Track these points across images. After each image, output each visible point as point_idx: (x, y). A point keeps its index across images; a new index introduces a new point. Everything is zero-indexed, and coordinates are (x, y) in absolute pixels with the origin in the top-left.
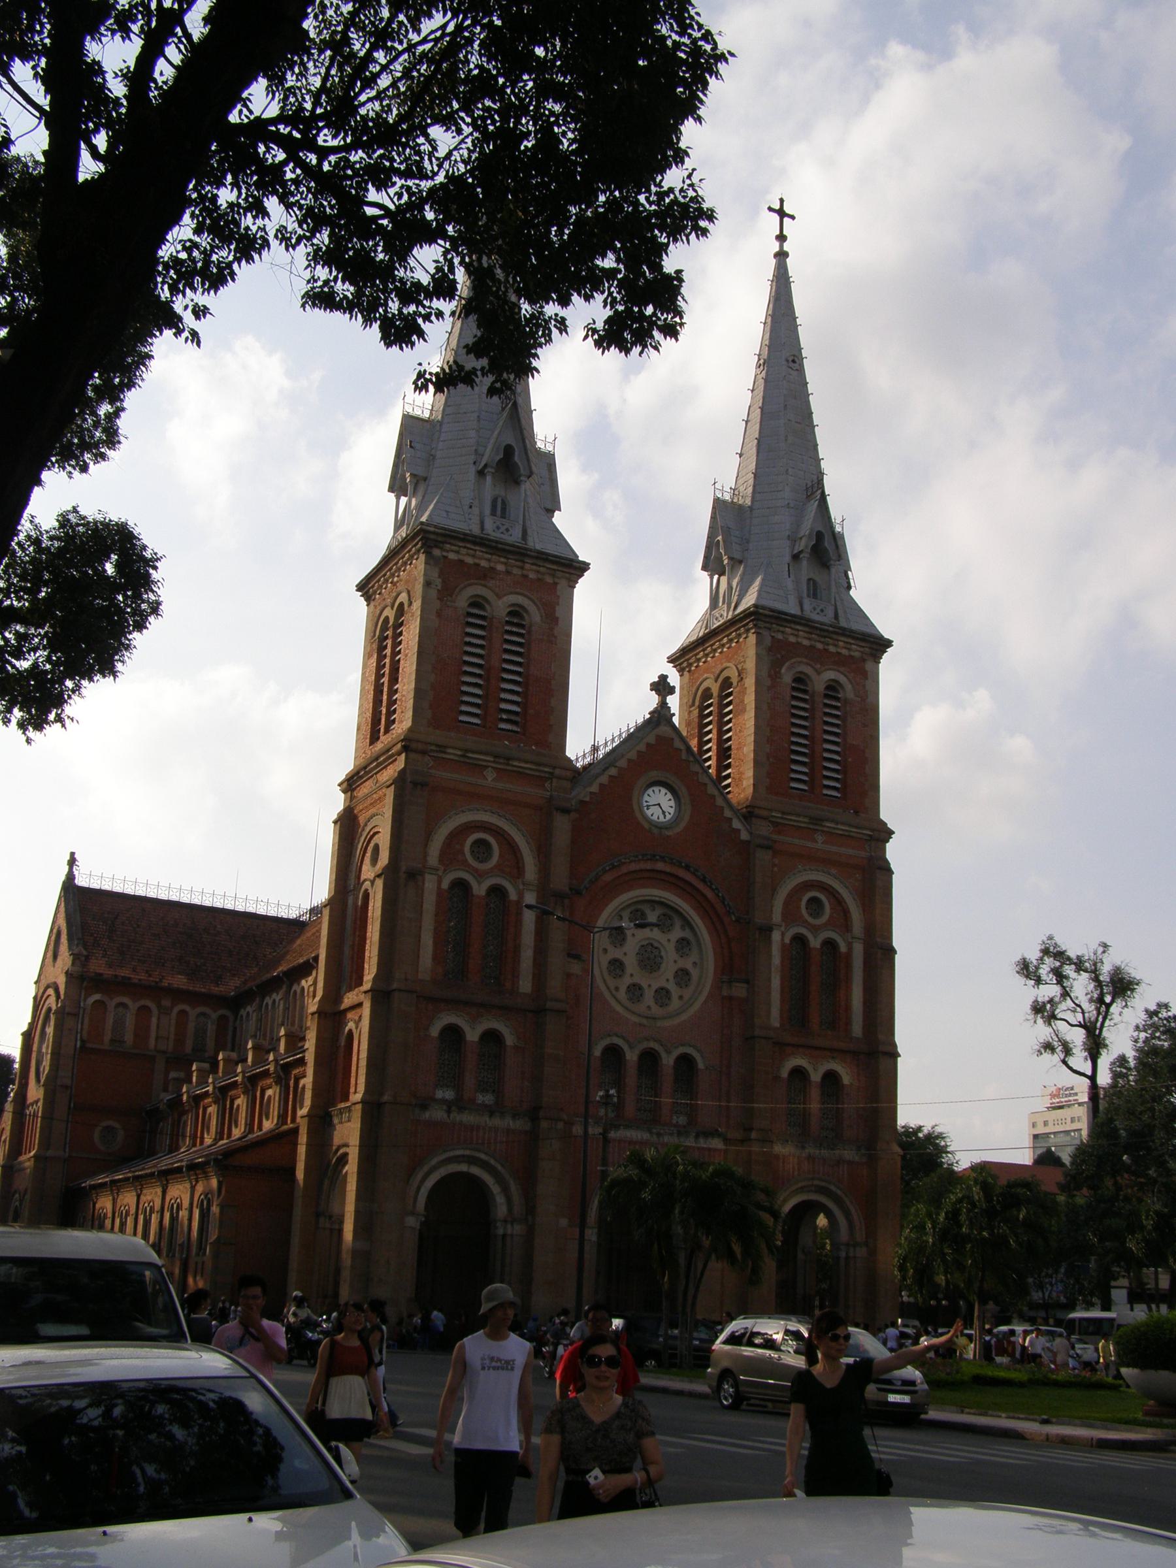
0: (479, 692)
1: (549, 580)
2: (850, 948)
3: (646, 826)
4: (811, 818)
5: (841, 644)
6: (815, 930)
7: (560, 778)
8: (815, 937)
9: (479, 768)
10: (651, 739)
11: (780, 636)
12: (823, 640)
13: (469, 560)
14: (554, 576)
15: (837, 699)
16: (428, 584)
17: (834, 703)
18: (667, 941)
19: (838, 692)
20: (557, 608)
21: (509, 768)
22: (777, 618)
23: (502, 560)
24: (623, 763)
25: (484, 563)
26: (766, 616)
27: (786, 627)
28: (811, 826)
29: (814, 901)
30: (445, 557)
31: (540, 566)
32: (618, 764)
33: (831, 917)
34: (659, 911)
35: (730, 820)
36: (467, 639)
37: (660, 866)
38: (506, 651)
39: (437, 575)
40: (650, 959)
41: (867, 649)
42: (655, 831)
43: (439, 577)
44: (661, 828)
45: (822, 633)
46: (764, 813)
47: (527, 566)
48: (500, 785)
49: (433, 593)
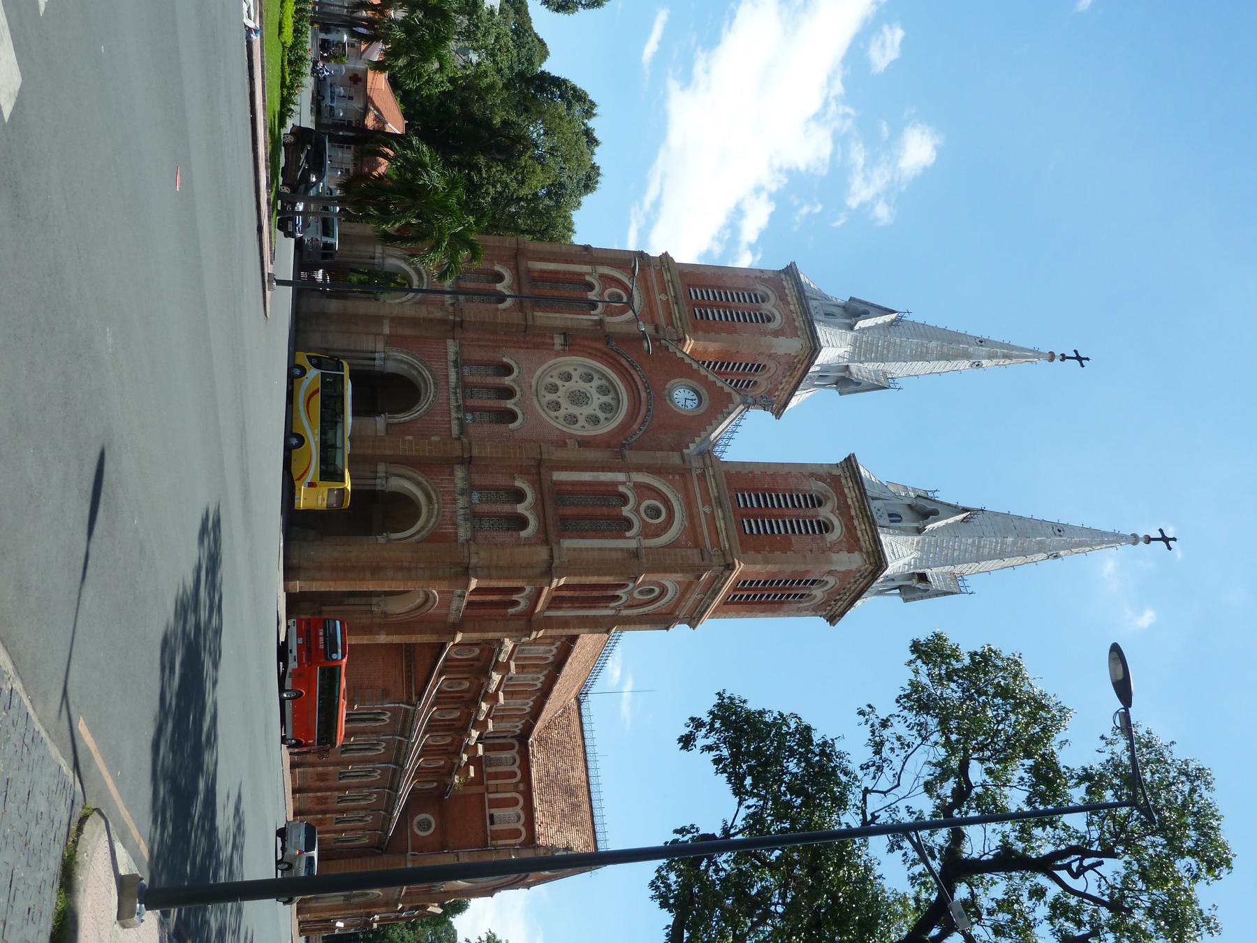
2: (630, 538)
3: (668, 386)
4: (719, 497)
6: (637, 511)
8: (630, 511)
9: (664, 290)
11: (844, 481)
17: (816, 528)
18: (593, 408)
19: (826, 532)
22: (855, 473)
26: (852, 466)
28: (713, 501)
29: (658, 515)
33: (653, 524)
34: (613, 403)
37: (643, 395)
40: (578, 398)
42: (666, 392)
45: (863, 510)
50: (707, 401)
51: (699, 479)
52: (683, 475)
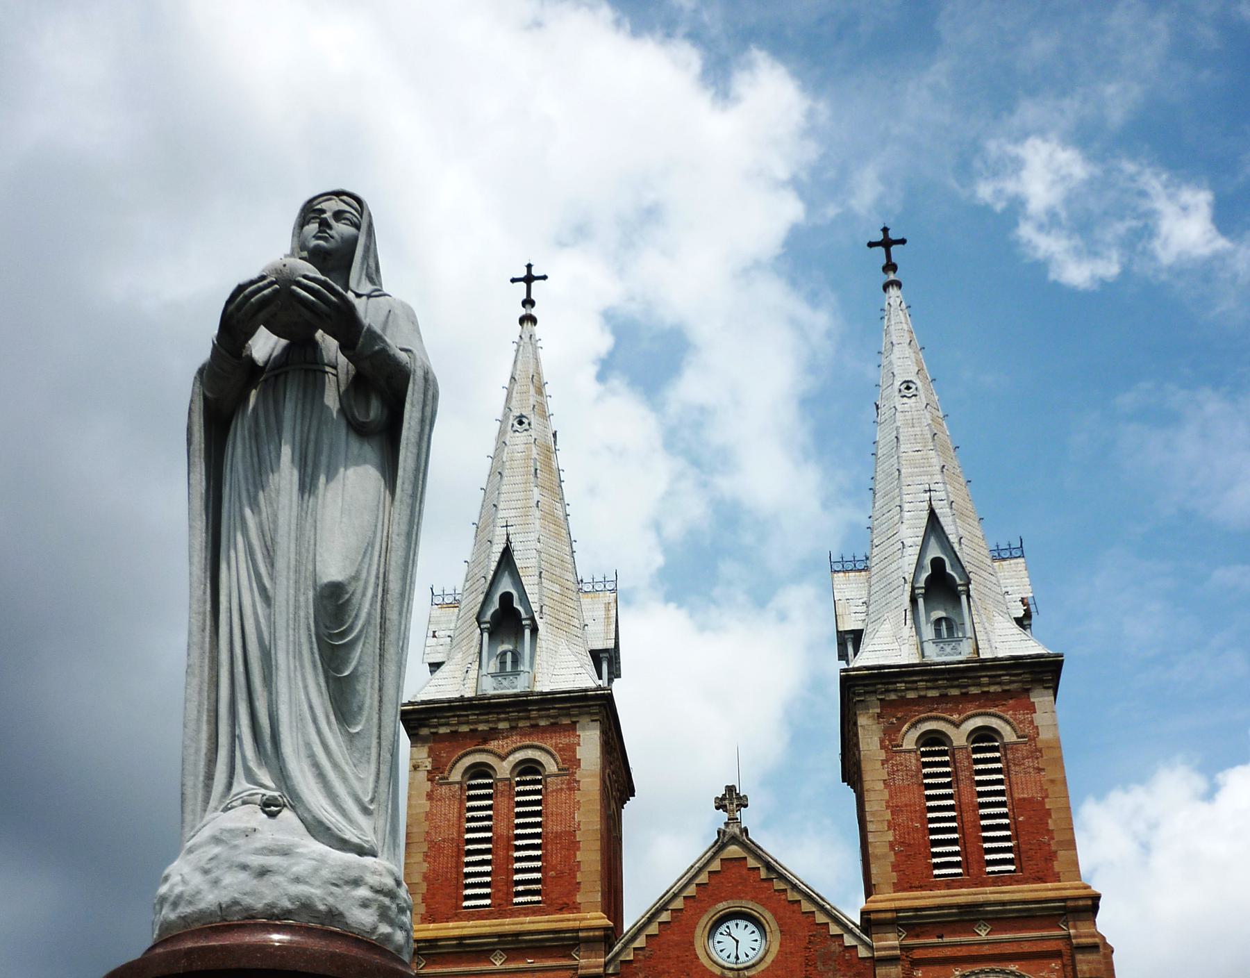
0: (488, 868)
1: (566, 721)
3: (717, 971)
4: (959, 906)
5: (985, 680)
7: (587, 941)
10: (716, 866)
11: (893, 697)
12: (956, 683)
13: (464, 729)
14: (569, 715)
15: (995, 749)
16: (415, 768)
17: (989, 755)
20: (577, 747)
21: (524, 945)
23: (503, 716)
24: (678, 904)
25: (481, 727)
27: (895, 683)
30: (436, 733)
31: (549, 709)
32: (671, 907)
35: (842, 935)
36: (469, 814)
38: (519, 815)
39: (426, 756)
41: (1026, 676)
43: (429, 756)
44: (738, 970)
45: (952, 675)
46: (883, 916)
47: (534, 714)
48: (513, 966)
49: (422, 775)
50: (744, 903)
51: (918, 936)
52: (916, 963)
